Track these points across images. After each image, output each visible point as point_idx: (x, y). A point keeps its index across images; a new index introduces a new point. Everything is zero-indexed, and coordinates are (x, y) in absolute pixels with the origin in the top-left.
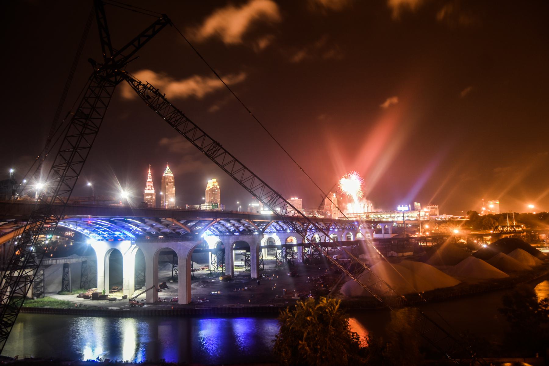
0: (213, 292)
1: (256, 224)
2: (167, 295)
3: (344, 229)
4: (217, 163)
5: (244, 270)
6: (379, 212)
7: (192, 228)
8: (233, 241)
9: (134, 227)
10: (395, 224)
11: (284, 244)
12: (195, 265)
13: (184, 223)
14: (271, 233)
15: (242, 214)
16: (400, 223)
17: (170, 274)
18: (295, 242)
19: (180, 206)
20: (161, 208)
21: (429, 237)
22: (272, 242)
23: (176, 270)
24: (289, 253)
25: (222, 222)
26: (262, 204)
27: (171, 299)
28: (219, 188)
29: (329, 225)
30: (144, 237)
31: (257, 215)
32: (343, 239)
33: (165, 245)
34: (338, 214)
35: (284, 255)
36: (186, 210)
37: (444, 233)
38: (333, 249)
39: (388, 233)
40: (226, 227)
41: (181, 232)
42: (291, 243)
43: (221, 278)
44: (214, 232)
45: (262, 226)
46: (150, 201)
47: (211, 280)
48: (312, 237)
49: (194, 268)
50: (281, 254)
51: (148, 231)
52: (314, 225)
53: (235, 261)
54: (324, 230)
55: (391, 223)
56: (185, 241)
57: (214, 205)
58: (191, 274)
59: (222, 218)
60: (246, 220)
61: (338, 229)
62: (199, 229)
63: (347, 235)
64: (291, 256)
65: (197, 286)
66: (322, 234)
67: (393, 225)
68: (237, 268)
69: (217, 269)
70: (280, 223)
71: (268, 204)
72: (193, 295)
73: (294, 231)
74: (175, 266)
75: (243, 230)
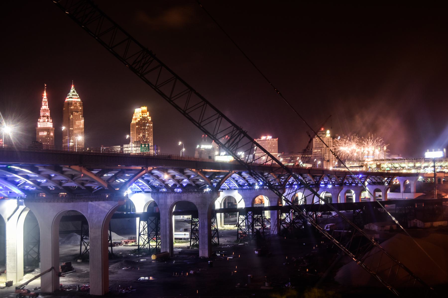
0: (142, 278)
1: (207, 176)
2: (73, 281)
3: (342, 185)
4: (148, 83)
5: (189, 245)
6: (397, 160)
7: (110, 181)
8: (173, 201)
9: (22, 178)
10: (420, 178)
11: (250, 206)
12: (115, 237)
13: (98, 172)
14: (230, 189)
15: (186, 161)
16: (429, 177)
17: (77, 250)
18: (267, 203)
19: (92, 148)
20: (64, 150)
22: (232, 203)
23: (85, 244)
24: (258, 220)
25: (156, 172)
26: (218, 146)
27: (79, 288)
28: (151, 121)
29: (320, 179)
30: (38, 194)
31: (209, 163)
32: (341, 200)
33: (69, 206)
34: (334, 161)
35: (249, 224)
36: (101, 153)
38: (324, 214)
39: (410, 192)
40: (162, 179)
41: (93, 187)
42: (260, 206)
43: (153, 257)
44: (143, 188)
45: (217, 179)
46: (46, 140)
47: (139, 260)
48: (294, 195)
49: (113, 242)
50: (245, 221)
51: (44, 185)
52: (296, 178)
53: (175, 231)
56: (100, 200)
57: (143, 146)
58: (109, 251)
59: (156, 166)
60: (192, 170)
61: (333, 185)
62: (121, 182)
63: (347, 194)
64: (260, 225)
65: (118, 268)
66: (308, 192)
67: (418, 180)
68: (179, 242)
69: (148, 242)
70: (244, 174)
71: (227, 146)
72: (112, 281)
73: (265, 187)
74: (84, 237)
75: (188, 185)
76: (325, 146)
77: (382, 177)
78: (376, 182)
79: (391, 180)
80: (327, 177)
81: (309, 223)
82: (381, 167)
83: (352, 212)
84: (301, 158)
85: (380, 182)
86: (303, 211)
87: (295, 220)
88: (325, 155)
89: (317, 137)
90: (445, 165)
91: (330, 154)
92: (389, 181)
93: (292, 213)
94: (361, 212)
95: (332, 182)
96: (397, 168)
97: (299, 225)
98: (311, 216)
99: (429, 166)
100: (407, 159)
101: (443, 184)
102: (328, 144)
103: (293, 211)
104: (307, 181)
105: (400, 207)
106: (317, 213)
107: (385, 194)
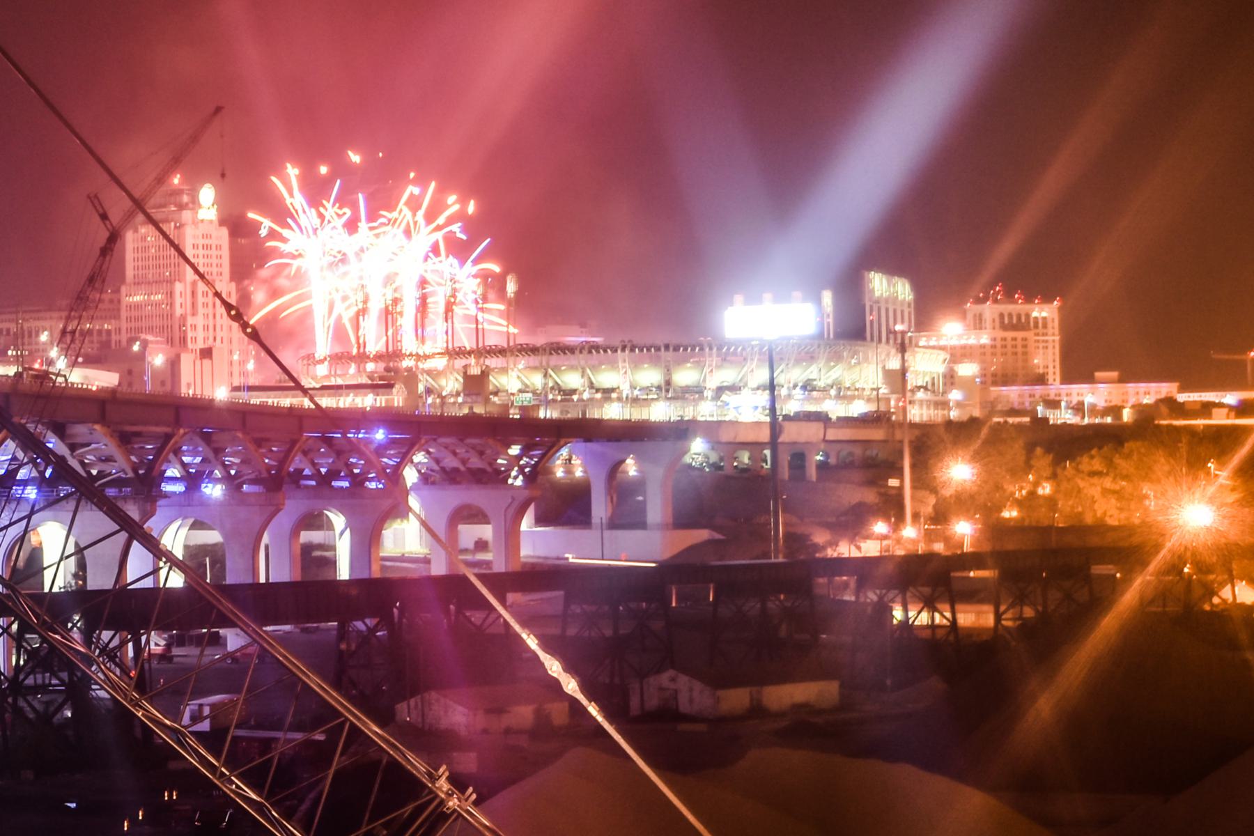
10: (698, 449)
21: (975, 560)
29: (159, 452)
34: (236, 357)
37: (1100, 528)
38: (180, 641)
39: (641, 524)
48: (22, 539)
52: (32, 445)
54: (111, 492)
55: (665, 439)
61: (234, 483)
63: (307, 536)
66: (95, 521)
67: (687, 459)
76: (190, 274)
77: (491, 441)
78: (462, 468)
79: (542, 457)
80: (198, 440)
81: (102, 694)
82: (491, 387)
83: (328, 630)
84: (57, 335)
85: (483, 471)
86: (70, 625)
87: (21, 677)
88: (190, 321)
89: (143, 224)
90: (829, 382)
91: (218, 316)
92: (527, 465)
93: (10, 635)
94: (378, 634)
95: (226, 468)
96: (575, 397)
97: (40, 702)
98: (111, 655)
99: (745, 385)
100: (629, 346)
101: (819, 479)
102: (206, 260)
103: (15, 627)
104: (91, 465)
105: (584, 606)
106: (144, 638)
107: (511, 536)
